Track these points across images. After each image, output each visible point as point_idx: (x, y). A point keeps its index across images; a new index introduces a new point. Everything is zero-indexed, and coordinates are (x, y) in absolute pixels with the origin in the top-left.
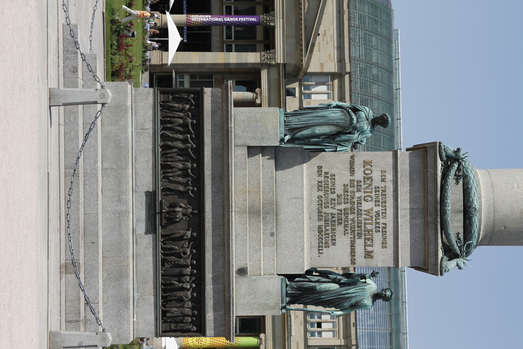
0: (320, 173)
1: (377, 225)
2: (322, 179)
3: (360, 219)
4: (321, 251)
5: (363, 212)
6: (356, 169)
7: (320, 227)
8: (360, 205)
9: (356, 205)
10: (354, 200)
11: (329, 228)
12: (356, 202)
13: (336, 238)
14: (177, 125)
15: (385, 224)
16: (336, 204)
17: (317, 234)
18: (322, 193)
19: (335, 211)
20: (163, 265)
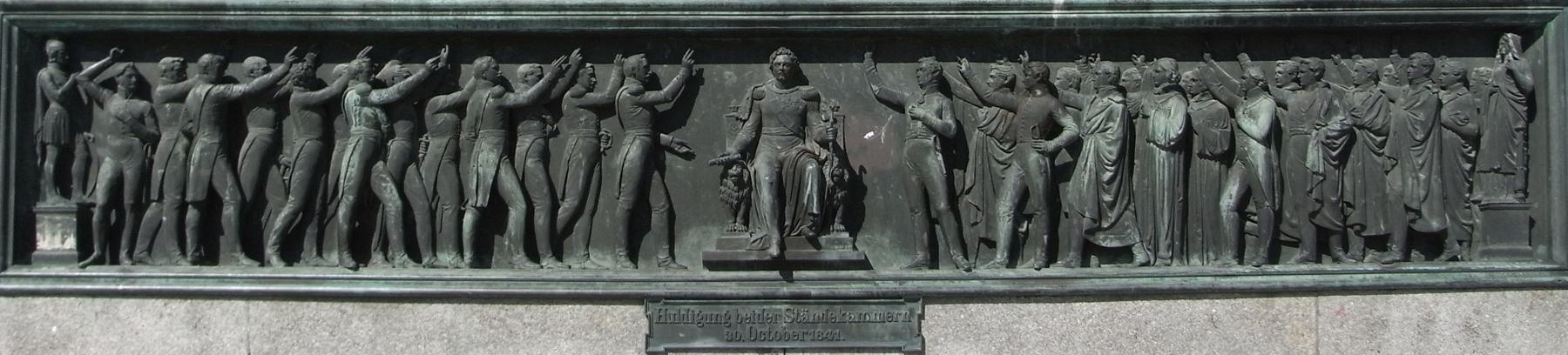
14: (222, 164)
20: (1122, 255)
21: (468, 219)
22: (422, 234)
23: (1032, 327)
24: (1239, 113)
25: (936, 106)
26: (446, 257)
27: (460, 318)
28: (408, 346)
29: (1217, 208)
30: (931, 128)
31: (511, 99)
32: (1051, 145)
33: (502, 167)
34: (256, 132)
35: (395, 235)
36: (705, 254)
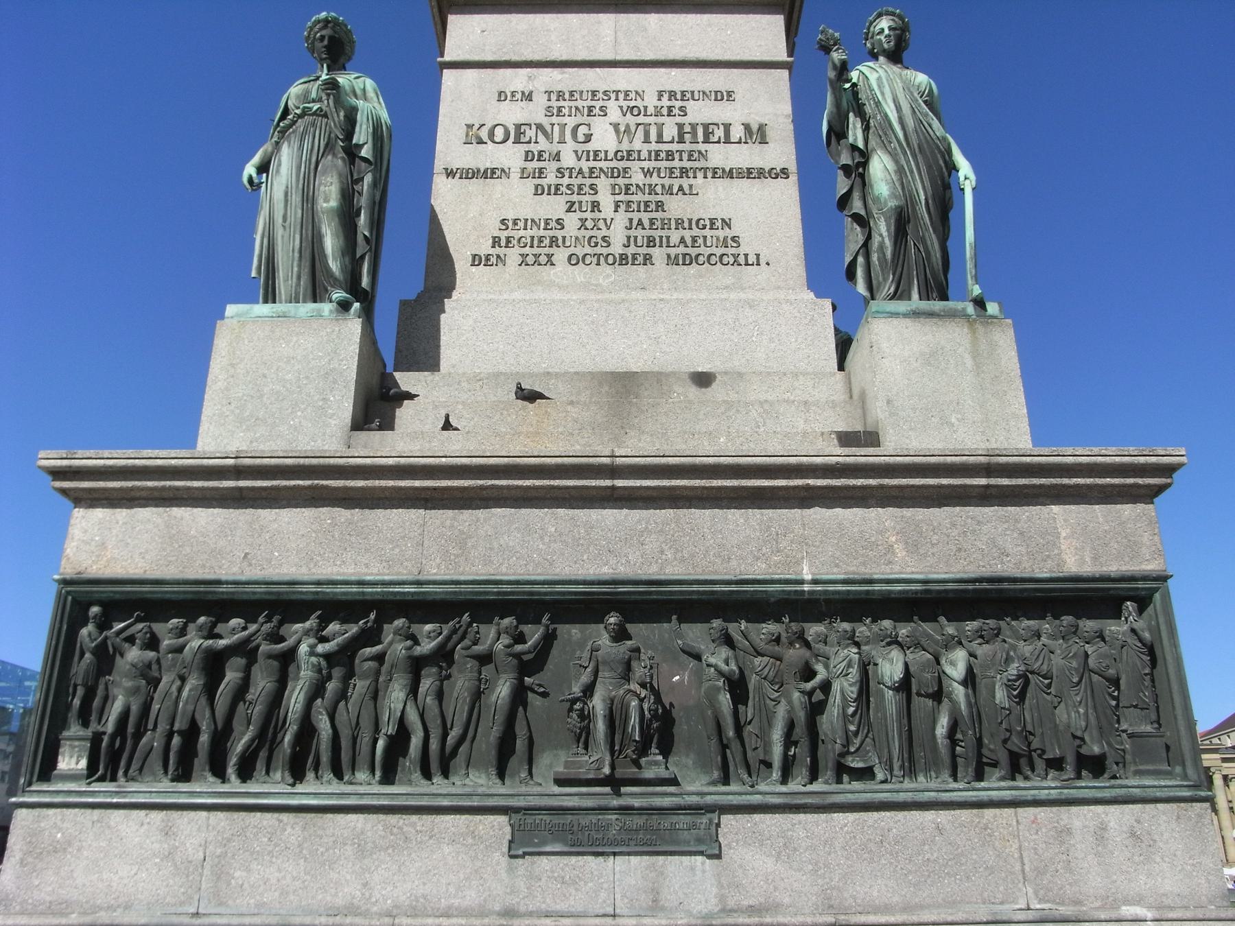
0: (493, 260)
1: (665, 111)
2: (513, 255)
3: (644, 154)
4: (752, 259)
5: (625, 146)
6: (488, 165)
7: (672, 261)
8: (602, 155)
9: (604, 165)
10: (586, 170)
11: (675, 237)
12: (592, 164)
13: (707, 216)
14: (203, 701)
15: (660, 95)
16: (597, 215)
17: (693, 269)
18: (561, 255)
19: (621, 219)
20: (866, 774)
21: (381, 744)
22: (345, 756)
23: (802, 834)
24: (943, 662)
25: (724, 656)
26: (362, 776)
27: (369, 826)
28: (327, 850)
29: (934, 736)
30: (720, 673)
31: (418, 650)
32: (809, 686)
33: (408, 704)
34: (231, 676)
35: (325, 758)
36: (556, 773)
